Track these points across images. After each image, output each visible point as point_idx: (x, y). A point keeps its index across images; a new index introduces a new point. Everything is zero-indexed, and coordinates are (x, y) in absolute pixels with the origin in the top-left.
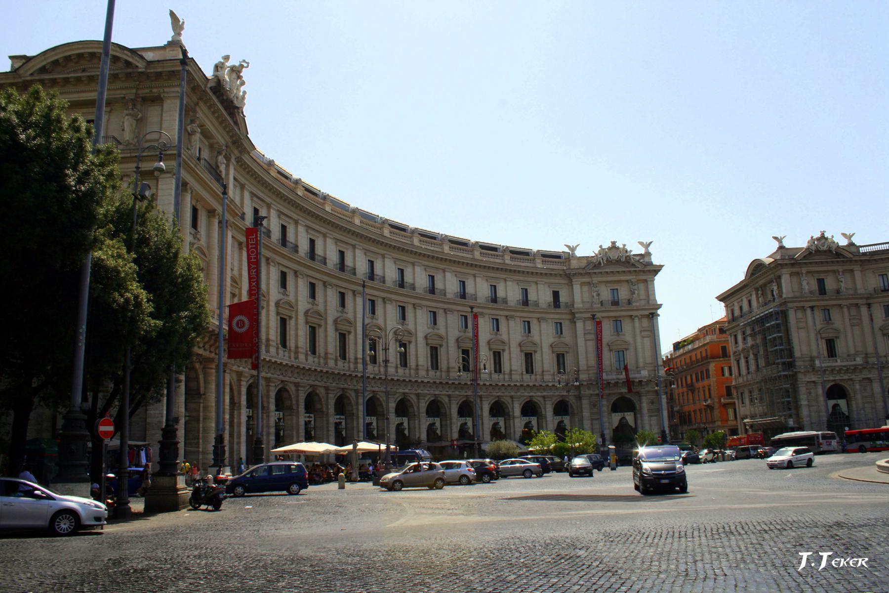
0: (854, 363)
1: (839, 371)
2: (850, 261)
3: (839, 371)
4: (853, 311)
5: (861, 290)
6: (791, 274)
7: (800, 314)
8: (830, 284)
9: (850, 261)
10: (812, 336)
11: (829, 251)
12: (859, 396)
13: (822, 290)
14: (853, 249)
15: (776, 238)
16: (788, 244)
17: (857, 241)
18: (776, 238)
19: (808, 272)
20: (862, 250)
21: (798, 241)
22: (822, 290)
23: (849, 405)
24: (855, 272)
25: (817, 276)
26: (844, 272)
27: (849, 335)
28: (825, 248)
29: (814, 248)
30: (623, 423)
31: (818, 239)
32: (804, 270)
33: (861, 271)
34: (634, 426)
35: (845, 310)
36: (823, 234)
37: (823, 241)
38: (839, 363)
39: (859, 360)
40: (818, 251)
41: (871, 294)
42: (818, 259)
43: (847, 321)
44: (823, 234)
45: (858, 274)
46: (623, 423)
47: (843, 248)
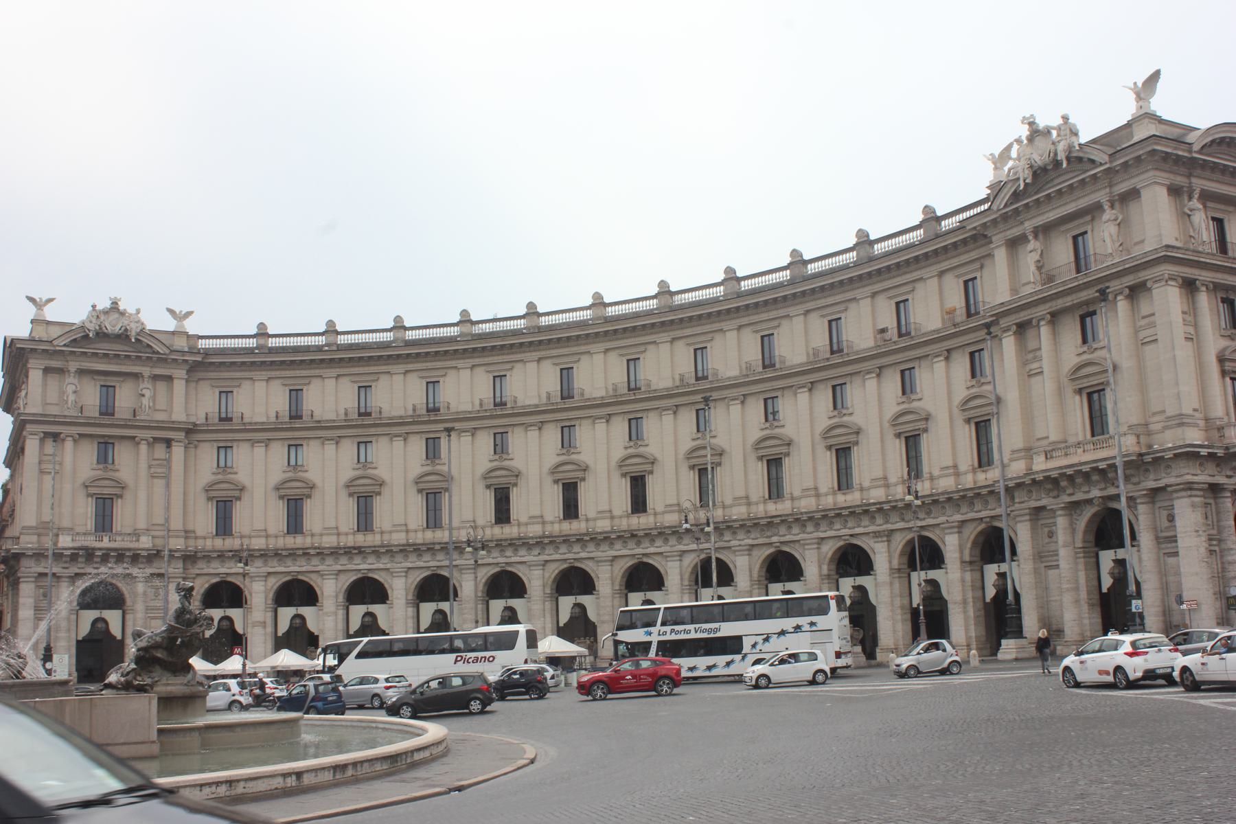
0: (132, 545)
1: (74, 558)
2: (163, 360)
3: (105, 558)
4: (160, 451)
5: (179, 415)
6: (47, 371)
7: (50, 447)
8: (125, 397)
9: (163, 360)
10: (68, 487)
11: (123, 337)
12: (140, 606)
13: (107, 410)
14: (181, 344)
15: (31, 300)
16: (50, 314)
17: (192, 327)
18: (31, 300)
19: (81, 372)
20: (202, 344)
21: (72, 310)
22: (107, 410)
23: (245, 617)
24: (176, 381)
25: (103, 380)
26: (155, 378)
27: (142, 495)
28: (117, 330)
29: (91, 326)
30: (100, 628)
31: (106, 312)
32: (73, 366)
33: (187, 381)
34: (119, 637)
35: (143, 447)
36: (115, 304)
37: (116, 315)
38: (106, 543)
39: (145, 542)
40: (102, 335)
41: (195, 425)
42: (104, 347)
43: (143, 465)
44: (115, 304)
45: (179, 386)
46: (100, 628)
47: (153, 334)
